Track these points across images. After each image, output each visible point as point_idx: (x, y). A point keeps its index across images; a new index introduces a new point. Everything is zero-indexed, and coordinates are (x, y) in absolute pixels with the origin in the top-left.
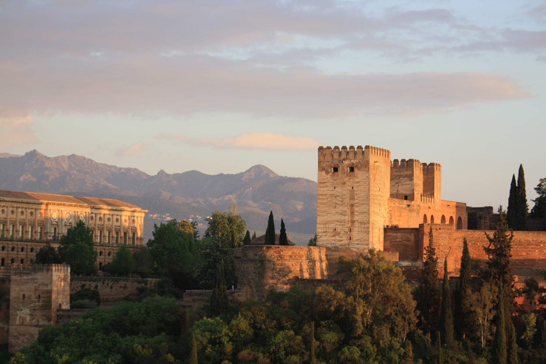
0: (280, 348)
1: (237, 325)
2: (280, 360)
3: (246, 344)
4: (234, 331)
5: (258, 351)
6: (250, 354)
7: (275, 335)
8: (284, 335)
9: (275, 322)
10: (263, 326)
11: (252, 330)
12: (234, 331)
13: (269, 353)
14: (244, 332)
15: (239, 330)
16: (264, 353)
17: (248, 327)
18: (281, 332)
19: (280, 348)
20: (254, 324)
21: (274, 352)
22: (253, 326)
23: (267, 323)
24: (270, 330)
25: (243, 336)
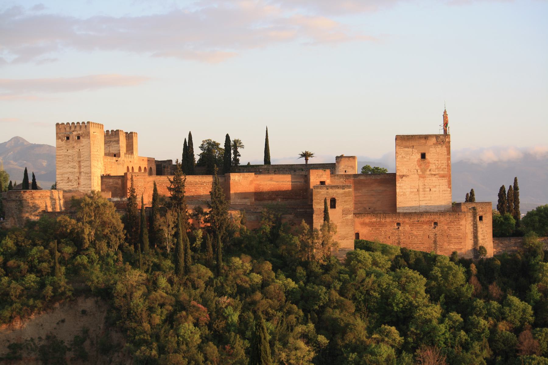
0: (35, 258)
1: (6, 244)
2: (35, 266)
3: (12, 256)
4: (4, 248)
5: (20, 260)
6: (15, 263)
7: (31, 249)
8: (37, 250)
9: (31, 241)
10: (23, 244)
11: (15, 247)
12: (4, 248)
13: (28, 261)
14: (11, 248)
15: (7, 247)
16: (24, 262)
17: (13, 245)
18: (35, 248)
19: (35, 258)
20: (17, 243)
21: (31, 261)
22: (16, 244)
23: (25, 242)
24: (28, 246)
25: (9, 251)
